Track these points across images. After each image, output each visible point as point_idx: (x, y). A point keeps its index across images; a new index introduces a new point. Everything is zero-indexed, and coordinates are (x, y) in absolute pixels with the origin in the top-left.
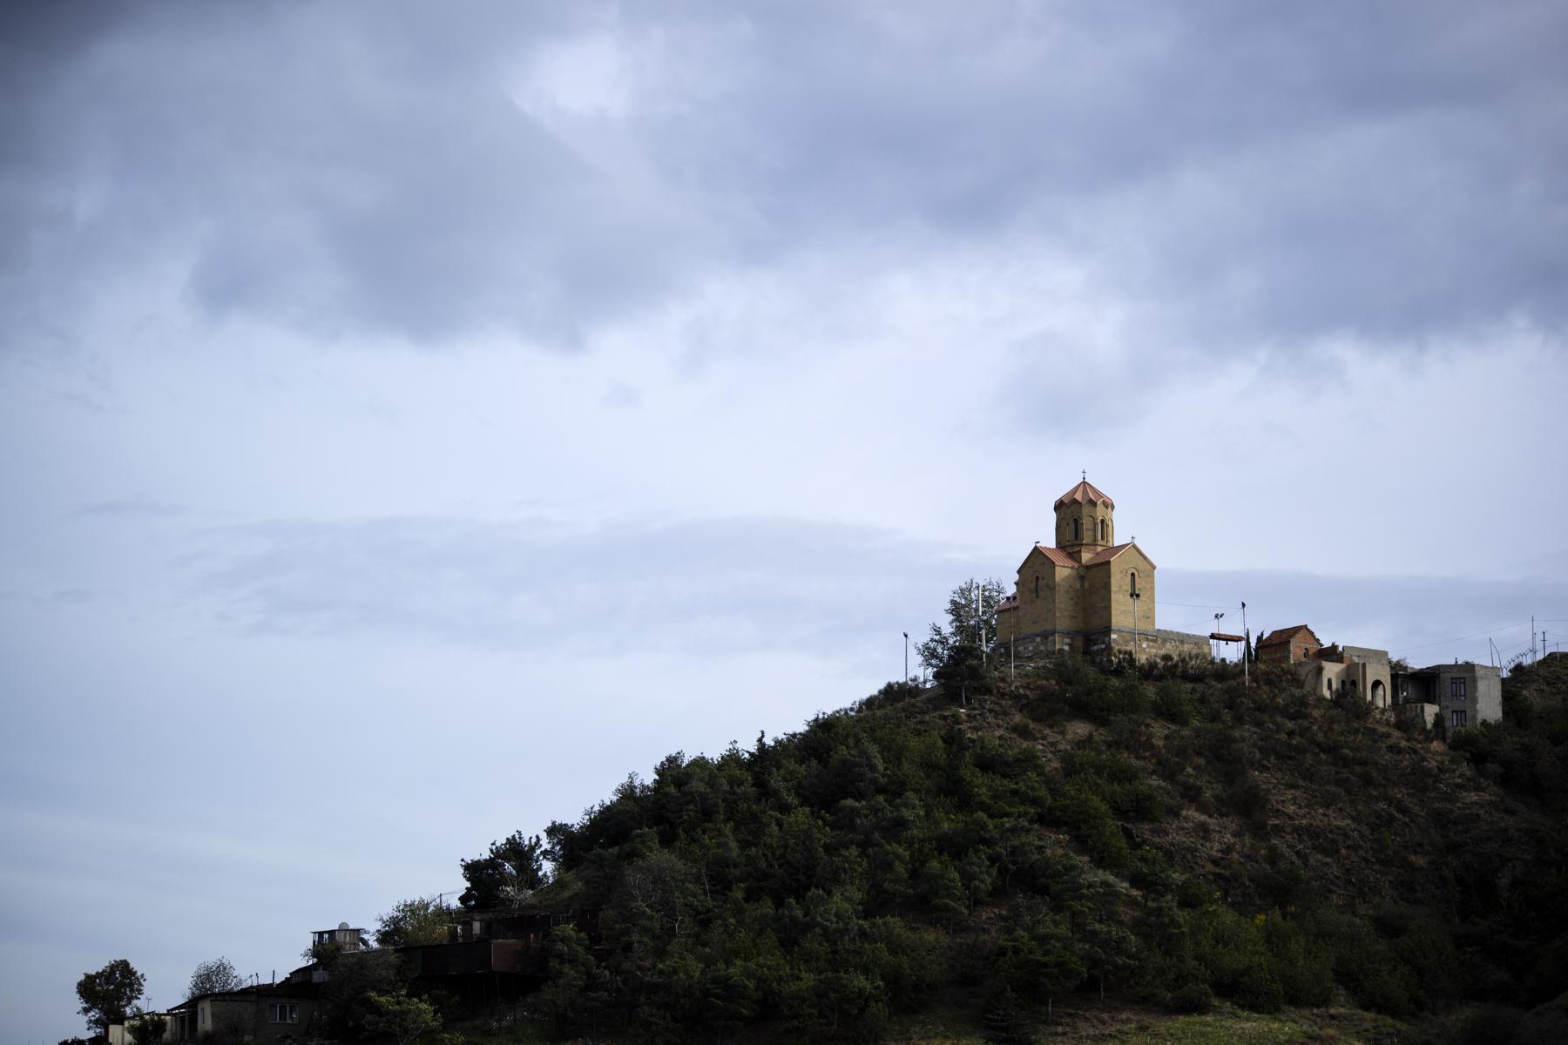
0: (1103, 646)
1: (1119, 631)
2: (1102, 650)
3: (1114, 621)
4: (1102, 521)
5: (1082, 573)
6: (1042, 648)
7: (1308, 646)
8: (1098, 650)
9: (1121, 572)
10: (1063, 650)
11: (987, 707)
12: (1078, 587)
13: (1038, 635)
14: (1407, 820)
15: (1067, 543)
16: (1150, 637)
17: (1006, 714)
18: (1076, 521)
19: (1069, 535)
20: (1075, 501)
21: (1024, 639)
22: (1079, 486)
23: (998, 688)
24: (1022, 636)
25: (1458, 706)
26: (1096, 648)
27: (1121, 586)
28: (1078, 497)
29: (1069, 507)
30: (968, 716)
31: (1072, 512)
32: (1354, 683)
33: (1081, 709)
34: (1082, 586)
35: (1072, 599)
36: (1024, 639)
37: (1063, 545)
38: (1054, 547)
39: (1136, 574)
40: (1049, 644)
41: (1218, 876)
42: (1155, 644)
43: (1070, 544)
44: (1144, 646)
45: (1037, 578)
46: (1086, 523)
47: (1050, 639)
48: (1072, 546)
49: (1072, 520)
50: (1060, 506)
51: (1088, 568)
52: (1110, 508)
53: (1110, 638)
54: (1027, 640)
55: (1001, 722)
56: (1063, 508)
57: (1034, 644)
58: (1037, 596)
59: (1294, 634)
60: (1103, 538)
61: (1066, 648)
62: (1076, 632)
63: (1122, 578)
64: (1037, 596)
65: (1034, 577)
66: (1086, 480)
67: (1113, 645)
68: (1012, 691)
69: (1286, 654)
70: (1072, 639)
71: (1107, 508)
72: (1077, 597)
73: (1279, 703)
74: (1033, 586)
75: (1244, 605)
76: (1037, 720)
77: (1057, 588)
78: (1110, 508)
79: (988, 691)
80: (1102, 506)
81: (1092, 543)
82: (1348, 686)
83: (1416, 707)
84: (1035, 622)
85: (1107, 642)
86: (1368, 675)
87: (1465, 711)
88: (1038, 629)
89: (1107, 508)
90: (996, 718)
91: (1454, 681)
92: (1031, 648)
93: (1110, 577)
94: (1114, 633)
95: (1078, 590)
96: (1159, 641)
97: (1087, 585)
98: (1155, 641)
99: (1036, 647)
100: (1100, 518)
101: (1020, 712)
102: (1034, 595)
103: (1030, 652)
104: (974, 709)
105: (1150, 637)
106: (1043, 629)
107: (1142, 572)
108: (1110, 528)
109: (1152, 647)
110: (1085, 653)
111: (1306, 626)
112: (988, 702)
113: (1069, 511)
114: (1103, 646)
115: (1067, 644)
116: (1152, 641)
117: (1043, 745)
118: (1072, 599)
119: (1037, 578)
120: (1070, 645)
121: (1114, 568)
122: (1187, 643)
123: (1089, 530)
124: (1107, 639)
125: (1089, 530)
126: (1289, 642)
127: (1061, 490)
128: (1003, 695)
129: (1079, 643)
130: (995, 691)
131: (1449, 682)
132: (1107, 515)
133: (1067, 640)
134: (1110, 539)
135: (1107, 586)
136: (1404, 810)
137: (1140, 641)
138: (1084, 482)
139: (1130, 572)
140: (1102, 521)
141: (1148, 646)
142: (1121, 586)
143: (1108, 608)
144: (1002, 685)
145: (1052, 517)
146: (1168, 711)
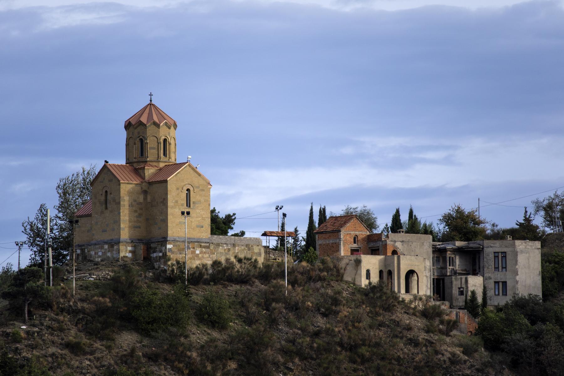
1: (175, 241)
3: (170, 232)
4: (165, 140)
5: (145, 188)
6: (109, 254)
7: (357, 233)
9: (178, 189)
11: (45, 324)
13: (106, 243)
18: (142, 141)
20: (141, 123)
23: (58, 303)
24: (93, 242)
27: (177, 202)
28: (144, 119)
29: (136, 128)
30: (28, 333)
31: (139, 133)
32: (390, 273)
34: (145, 199)
36: (95, 244)
39: (191, 189)
42: (208, 250)
47: (115, 247)
48: (138, 162)
50: (128, 126)
52: (172, 128)
55: (56, 338)
59: (345, 223)
60: (165, 154)
62: (138, 240)
64: (106, 208)
67: (168, 254)
68: (70, 306)
72: (141, 209)
73: (308, 305)
74: (103, 198)
76: (90, 333)
77: (122, 203)
78: (172, 128)
79: (48, 306)
82: (385, 275)
84: (104, 231)
89: (169, 128)
90: (52, 334)
92: (100, 254)
93: (167, 194)
95: (141, 203)
96: (212, 247)
97: (149, 199)
98: (208, 247)
99: (104, 253)
101: (76, 326)
102: (104, 206)
103: (100, 257)
104: (34, 326)
106: (110, 238)
109: (205, 253)
110: (147, 258)
113: (136, 131)
114: (161, 254)
116: (205, 247)
117: (90, 360)
118: (136, 211)
122: (238, 245)
126: (340, 231)
128: (62, 310)
130: (56, 307)
132: (169, 134)
135: (164, 201)
138: (151, 104)
139: (185, 188)
140: (165, 140)
141: (200, 253)
142: (177, 202)
144: (62, 300)
145: (123, 134)
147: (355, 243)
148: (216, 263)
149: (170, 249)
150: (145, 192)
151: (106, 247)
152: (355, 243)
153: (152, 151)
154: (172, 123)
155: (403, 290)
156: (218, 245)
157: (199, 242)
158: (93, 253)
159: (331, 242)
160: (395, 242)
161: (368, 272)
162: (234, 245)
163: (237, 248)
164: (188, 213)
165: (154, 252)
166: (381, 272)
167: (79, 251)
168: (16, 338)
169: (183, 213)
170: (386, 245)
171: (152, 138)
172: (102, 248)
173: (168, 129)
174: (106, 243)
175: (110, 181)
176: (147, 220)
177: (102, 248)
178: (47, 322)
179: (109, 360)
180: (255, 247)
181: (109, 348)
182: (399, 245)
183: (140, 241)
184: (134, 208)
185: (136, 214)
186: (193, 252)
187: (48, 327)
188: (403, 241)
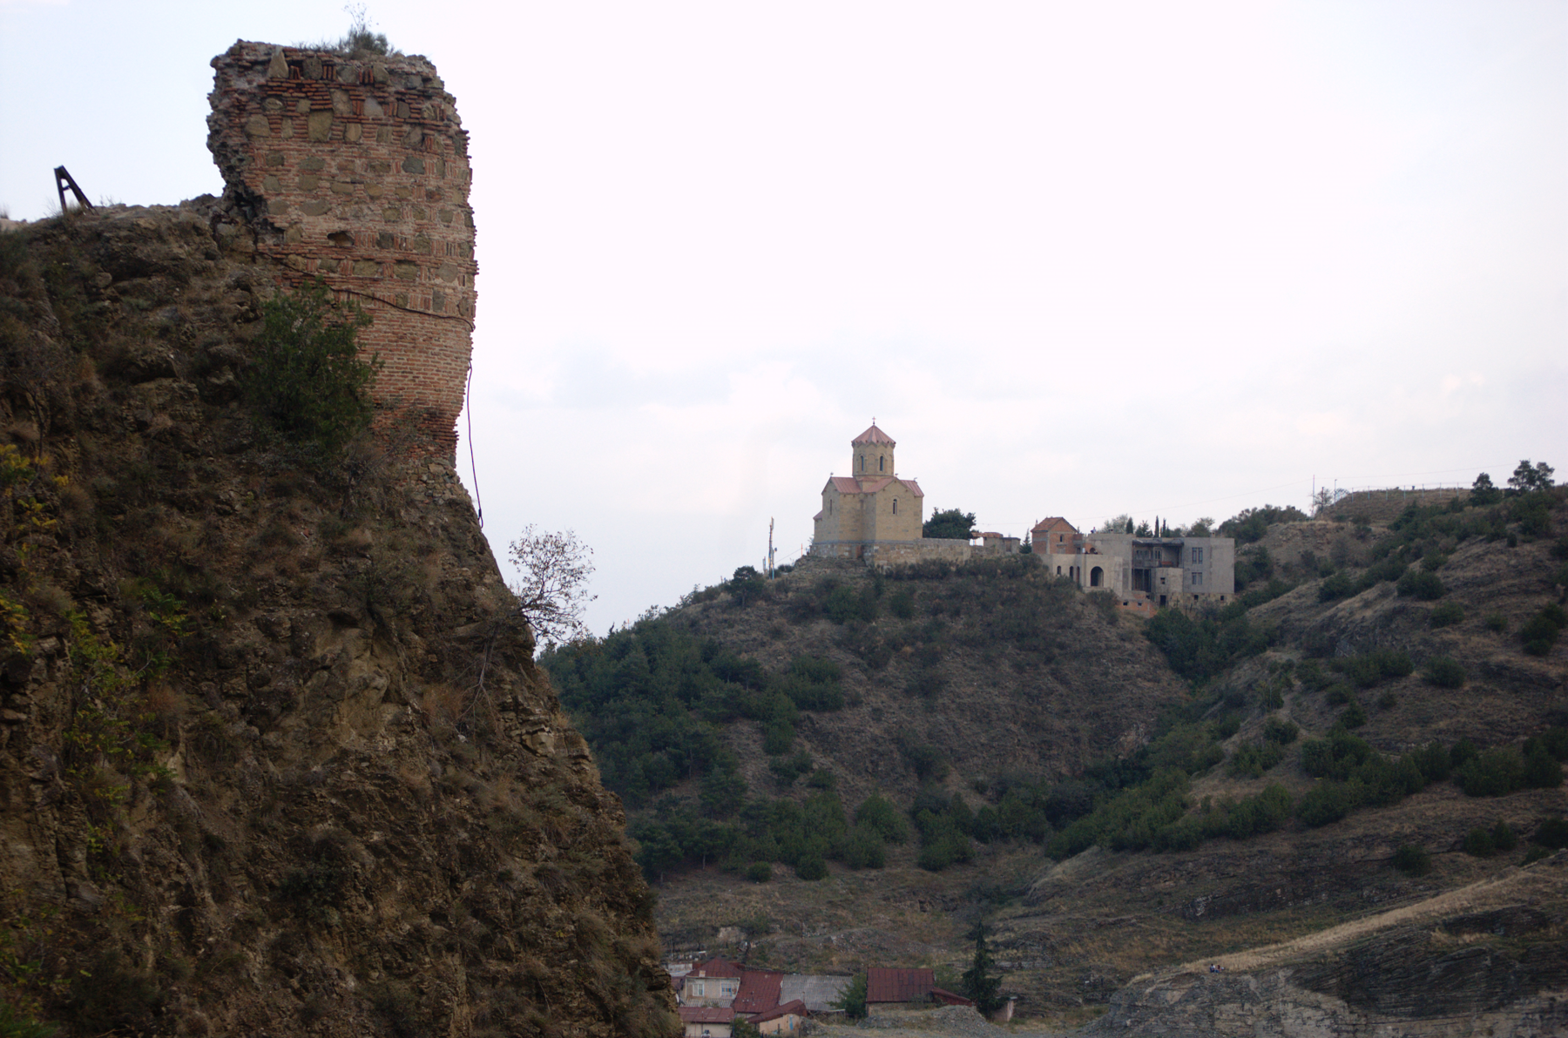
4: (882, 458)
25: (1196, 567)
28: (864, 441)
32: (1078, 568)
33: (826, 612)
34: (862, 507)
41: (872, 751)
50: (854, 444)
60: (881, 469)
108: (889, 462)
110: (861, 557)
120: (850, 552)
129: (855, 551)
133: (848, 549)
140: (882, 458)
146: (902, 610)
149: (876, 551)
157: (905, 545)
161: (1059, 568)
166: (1071, 568)
186: (898, 553)
188: (1102, 541)
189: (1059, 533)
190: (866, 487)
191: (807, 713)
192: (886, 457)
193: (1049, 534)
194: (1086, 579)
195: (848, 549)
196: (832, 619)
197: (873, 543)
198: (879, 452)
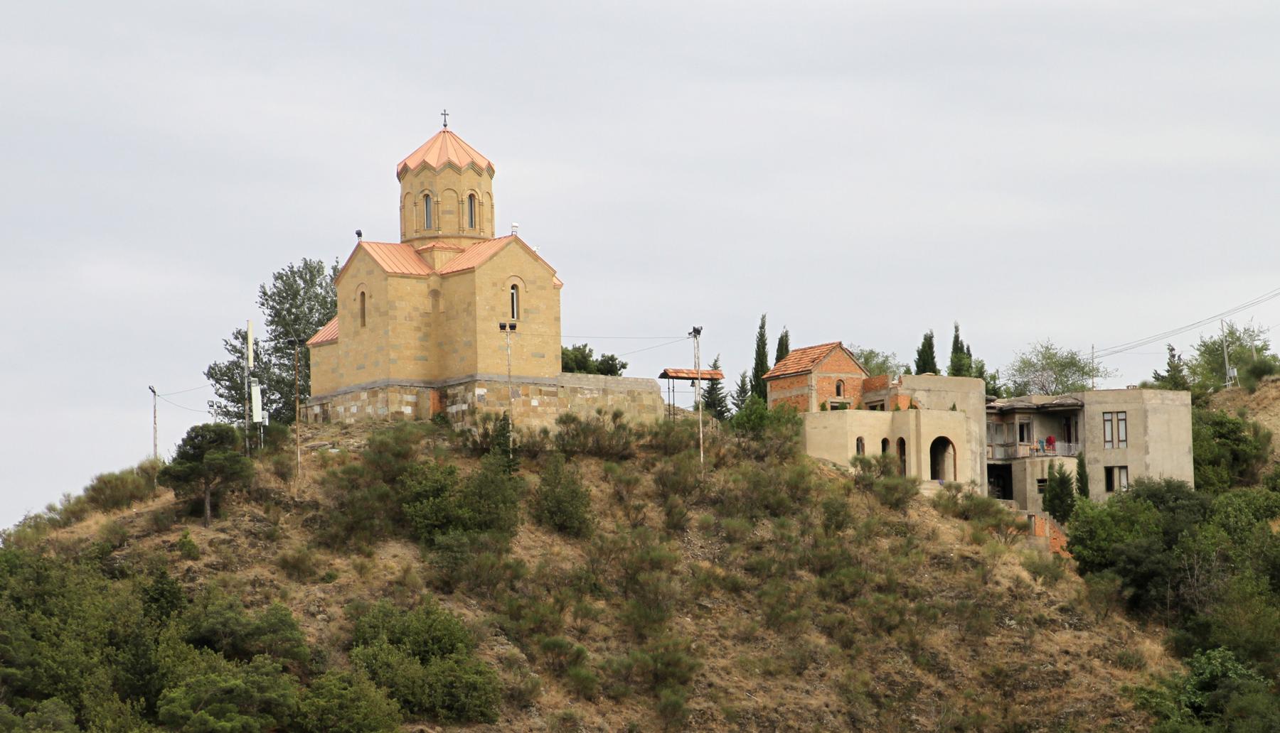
0: (465, 407)
2: (463, 412)
4: (471, 197)
6: (369, 410)
7: (843, 376)
8: (457, 413)
9: (495, 284)
10: (402, 413)
12: (429, 308)
13: (364, 389)
14: (940, 685)
15: (415, 235)
16: (544, 389)
17: (271, 537)
19: (416, 221)
20: (425, 166)
21: (346, 393)
22: (435, 139)
24: (343, 388)
26: (453, 409)
27: (493, 309)
28: (433, 160)
29: (417, 175)
31: (422, 183)
32: (902, 443)
34: (435, 306)
35: (418, 329)
36: (346, 393)
37: (408, 237)
38: (397, 239)
39: (520, 285)
40: (379, 405)
42: (554, 399)
43: (418, 235)
44: (535, 403)
45: (363, 294)
46: (446, 202)
47: (381, 395)
49: (421, 195)
50: (403, 173)
51: (444, 276)
52: (485, 175)
53: (474, 395)
54: (349, 396)
56: (409, 177)
57: (359, 404)
58: (363, 324)
60: (472, 224)
61: (408, 410)
62: (425, 382)
63: (495, 295)
64: (363, 324)
65: (359, 293)
66: (448, 128)
67: (477, 405)
69: (806, 390)
70: (417, 394)
71: (480, 175)
72: (428, 325)
74: (357, 306)
75: (697, 332)
77: (391, 313)
78: (485, 175)
80: (471, 172)
81: (455, 233)
82: (893, 450)
83: (1042, 462)
84: (360, 368)
85: (470, 401)
86: (923, 430)
87: (1125, 468)
88: (365, 378)
90: (253, 545)
91: (1108, 417)
92: (354, 410)
93: (474, 294)
94: (481, 386)
97: (442, 307)
98: (555, 394)
99: (361, 409)
100: (469, 192)
102: (359, 321)
103: (353, 415)
105: (544, 389)
106: (370, 380)
107: (534, 282)
108: (486, 208)
109: (549, 404)
111: (840, 343)
112: (247, 518)
115: (408, 404)
116: (548, 394)
118: (418, 329)
119: (363, 294)
120: (416, 405)
121: (481, 278)
122: (613, 393)
123: (450, 212)
124: (469, 395)
125: (450, 212)
126: (809, 372)
127: (404, 149)
131: (1099, 419)
132: (479, 185)
133: (410, 398)
134: (486, 226)
135: (470, 308)
136: (942, 670)
137: (527, 395)
140: (471, 197)
141: (540, 405)
142: (493, 309)
143: (472, 345)
147: (838, 394)
148: (566, 420)
149: (481, 398)
150: (435, 294)
151: (364, 395)
152: (838, 394)
153: (448, 217)
154: (484, 165)
155: (926, 473)
156: (574, 391)
157: (537, 385)
158: (340, 409)
159: (794, 393)
160: (914, 390)
161: (860, 441)
162: (605, 392)
163: (610, 397)
164: (513, 327)
165: (453, 403)
166: (885, 442)
167: (317, 410)
168: (191, 552)
169: (503, 327)
170: (896, 395)
171: (447, 193)
172: (357, 398)
173: (476, 176)
174: (364, 389)
175: (370, 273)
176: (440, 345)
177: (357, 398)
178: (246, 524)
179: (359, 592)
180: (644, 396)
181: (361, 570)
182: (920, 396)
183: (429, 385)
184: (415, 324)
185: (420, 334)
186: (527, 403)
187: (249, 533)
189: (835, 376)
190: (444, 261)
191: (420, 727)
192: (480, 196)
193: (814, 379)
194: (919, 463)
195: (410, 398)
196: (415, 539)
197: (470, 382)
198: (467, 183)
